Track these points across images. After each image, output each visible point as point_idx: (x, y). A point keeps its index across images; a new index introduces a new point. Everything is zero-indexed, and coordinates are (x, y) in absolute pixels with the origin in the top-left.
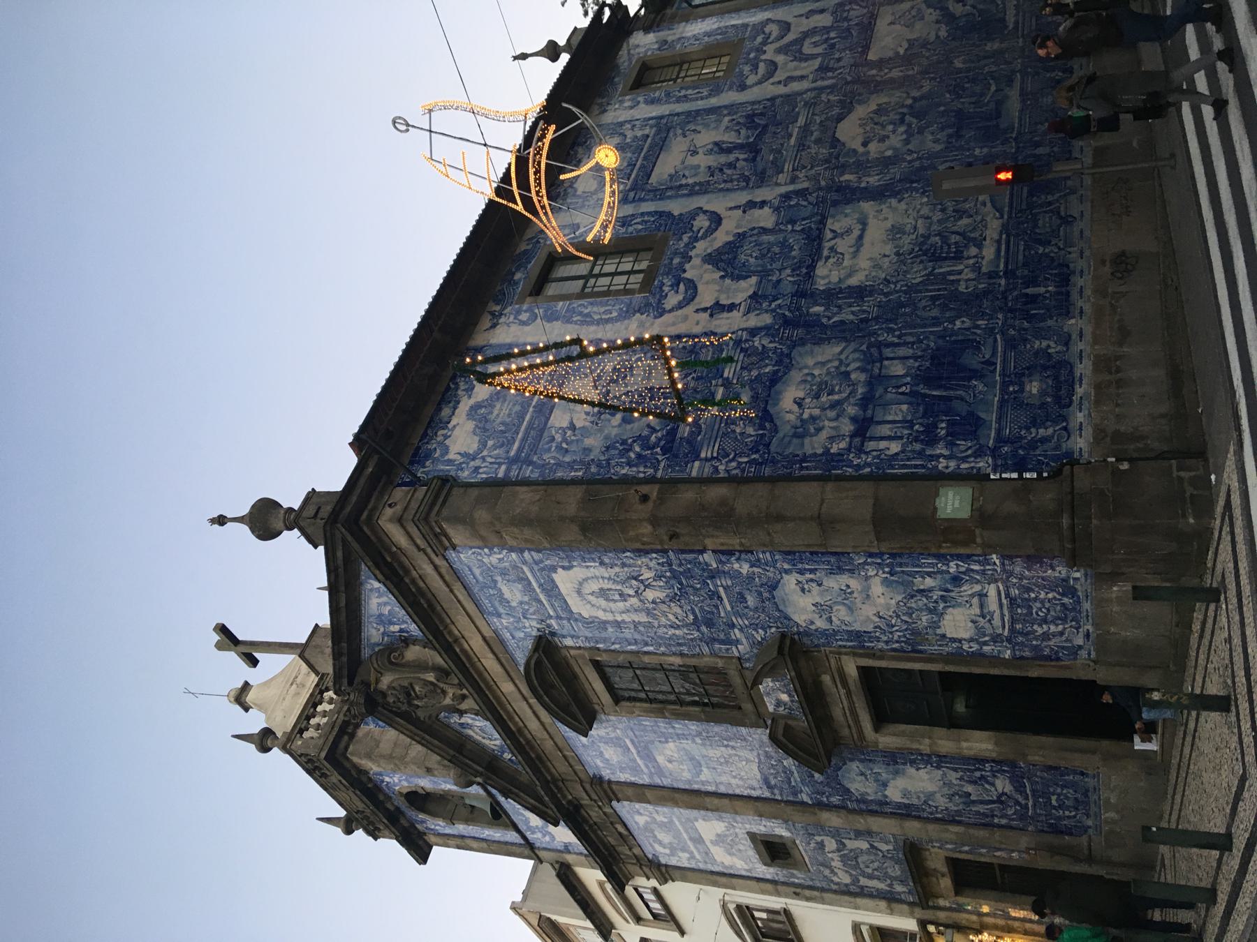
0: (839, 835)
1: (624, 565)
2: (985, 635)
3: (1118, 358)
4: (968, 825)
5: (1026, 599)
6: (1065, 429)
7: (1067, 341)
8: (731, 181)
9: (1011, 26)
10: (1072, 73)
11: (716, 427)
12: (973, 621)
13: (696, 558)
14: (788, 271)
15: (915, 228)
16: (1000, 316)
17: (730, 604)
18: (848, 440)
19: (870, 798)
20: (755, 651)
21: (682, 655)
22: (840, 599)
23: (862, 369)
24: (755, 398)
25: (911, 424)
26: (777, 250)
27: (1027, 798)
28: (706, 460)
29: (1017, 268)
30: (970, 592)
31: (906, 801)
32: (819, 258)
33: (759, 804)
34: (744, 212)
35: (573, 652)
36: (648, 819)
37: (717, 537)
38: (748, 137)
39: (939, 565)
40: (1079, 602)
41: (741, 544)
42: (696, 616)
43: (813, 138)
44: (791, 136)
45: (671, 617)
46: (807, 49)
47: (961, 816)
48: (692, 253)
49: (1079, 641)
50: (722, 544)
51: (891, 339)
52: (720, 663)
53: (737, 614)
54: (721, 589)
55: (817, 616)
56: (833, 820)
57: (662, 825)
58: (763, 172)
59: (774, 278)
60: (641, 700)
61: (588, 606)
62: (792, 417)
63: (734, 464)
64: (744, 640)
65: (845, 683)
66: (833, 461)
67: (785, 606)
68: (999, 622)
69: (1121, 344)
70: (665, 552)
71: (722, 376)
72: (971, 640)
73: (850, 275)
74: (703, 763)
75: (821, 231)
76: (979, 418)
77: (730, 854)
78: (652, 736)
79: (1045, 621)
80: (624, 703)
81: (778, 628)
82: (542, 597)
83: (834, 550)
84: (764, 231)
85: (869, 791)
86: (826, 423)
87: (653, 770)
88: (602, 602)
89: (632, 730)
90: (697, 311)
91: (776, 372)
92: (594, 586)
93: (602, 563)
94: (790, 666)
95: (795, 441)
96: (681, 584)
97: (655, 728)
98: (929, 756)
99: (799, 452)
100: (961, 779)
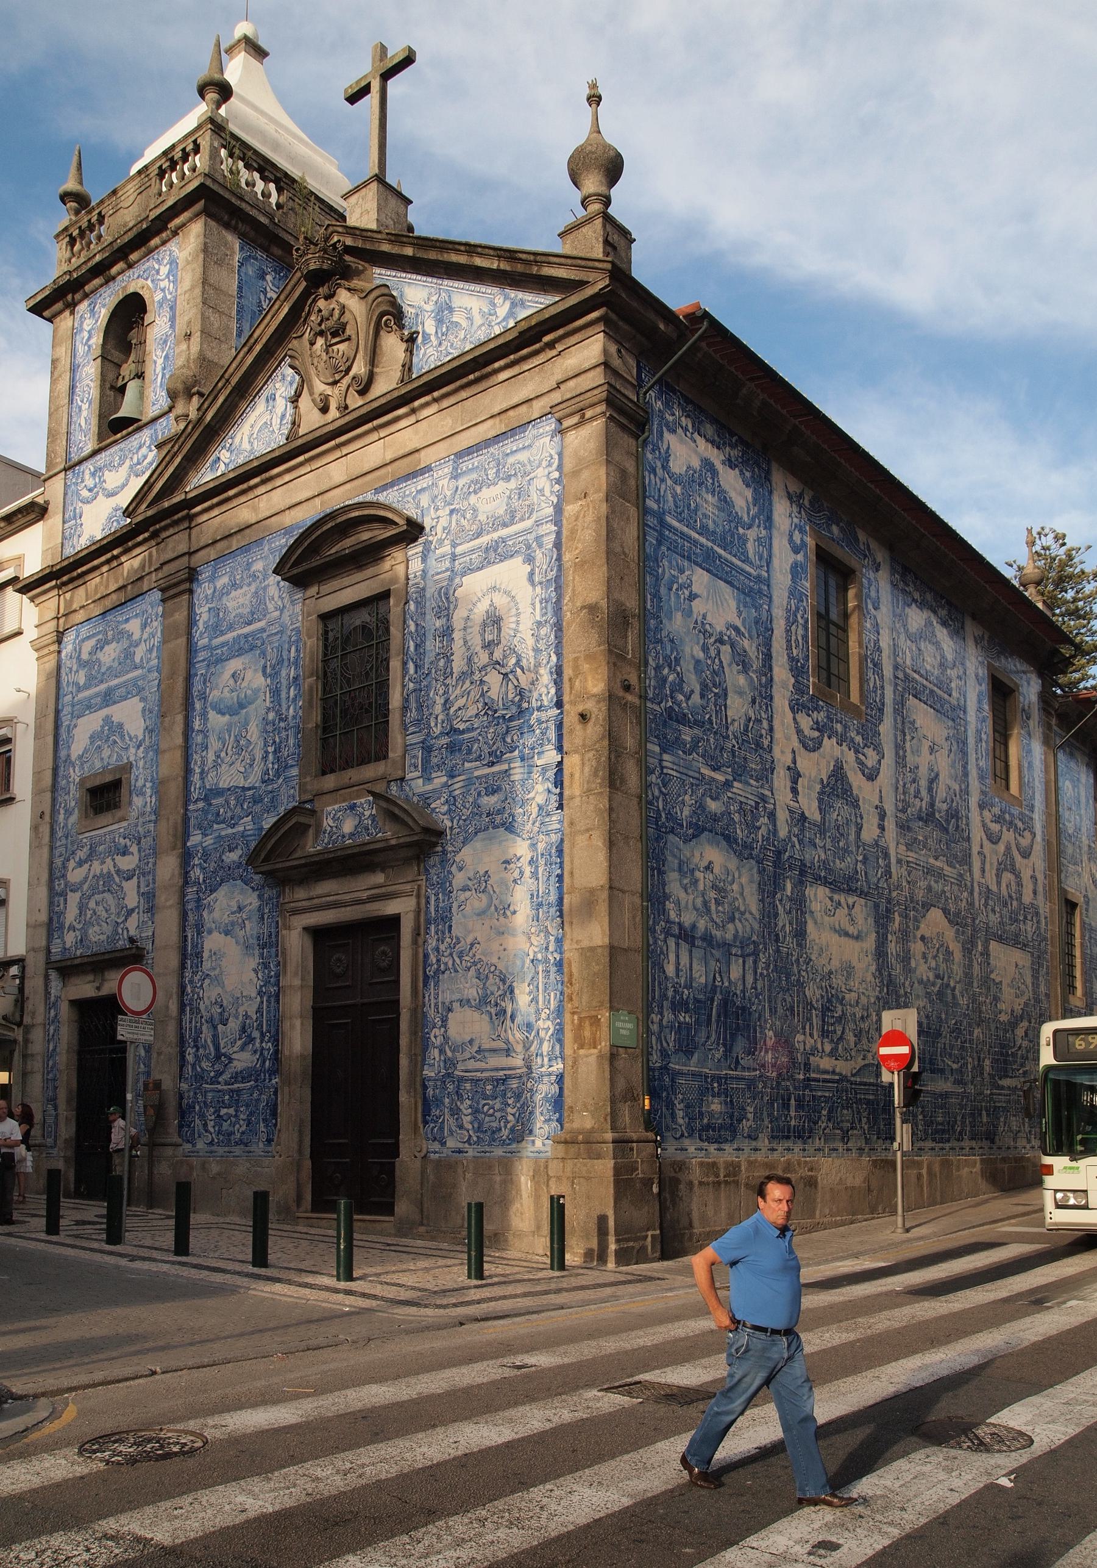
2: (453, 1051)
3: (737, 1183)
6: (682, 1135)
7: (752, 1137)
8: (904, 793)
9: (1000, 1082)
10: (958, 1140)
11: (691, 773)
12: (471, 1042)
13: (549, 741)
14: (823, 857)
15: (850, 991)
16: (774, 1074)
17: (486, 776)
18: (677, 920)
20: (415, 799)
21: (405, 709)
23: (735, 936)
24: (715, 818)
25: (689, 986)
26: (841, 844)
28: (661, 760)
29: (811, 1091)
32: (833, 891)
34: (877, 807)
36: (136, 637)
37: (582, 771)
38: (940, 812)
39: (548, 1011)
40: (503, 1143)
41: (572, 798)
42: (463, 732)
43: (932, 883)
44: (936, 859)
45: (461, 702)
46: (1007, 876)
48: (845, 747)
49: (451, 1143)
50: (572, 775)
51: (761, 965)
52: (394, 754)
53: (469, 782)
55: (471, 875)
56: (168, 867)
57: (128, 654)
58: (909, 829)
59: (817, 841)
60: (326, 647)
62: (696, 860)
63: (657, 793)
64: (429, 787)
66: (659, 903)
67: (484, 839)
68: (467, 1066)
69: (747, 1185)
71: (735, 780)
72: (446, 1038)
73: (816, 923)
75: (850, 891)
76: (692, 1054)
78: (272, 655)
79: (476, 1111)
80: (321, 626)
81: (451, 828)
84: (859, 828)
86: (692, 897)
87: (219, 651)
89: (281, 632)
90: (794, 752)
91: (736, 840)
94: (402, 840)
95: (676, 861)
96: (511, 719)
97: (286, 663)
99: (666, 868)
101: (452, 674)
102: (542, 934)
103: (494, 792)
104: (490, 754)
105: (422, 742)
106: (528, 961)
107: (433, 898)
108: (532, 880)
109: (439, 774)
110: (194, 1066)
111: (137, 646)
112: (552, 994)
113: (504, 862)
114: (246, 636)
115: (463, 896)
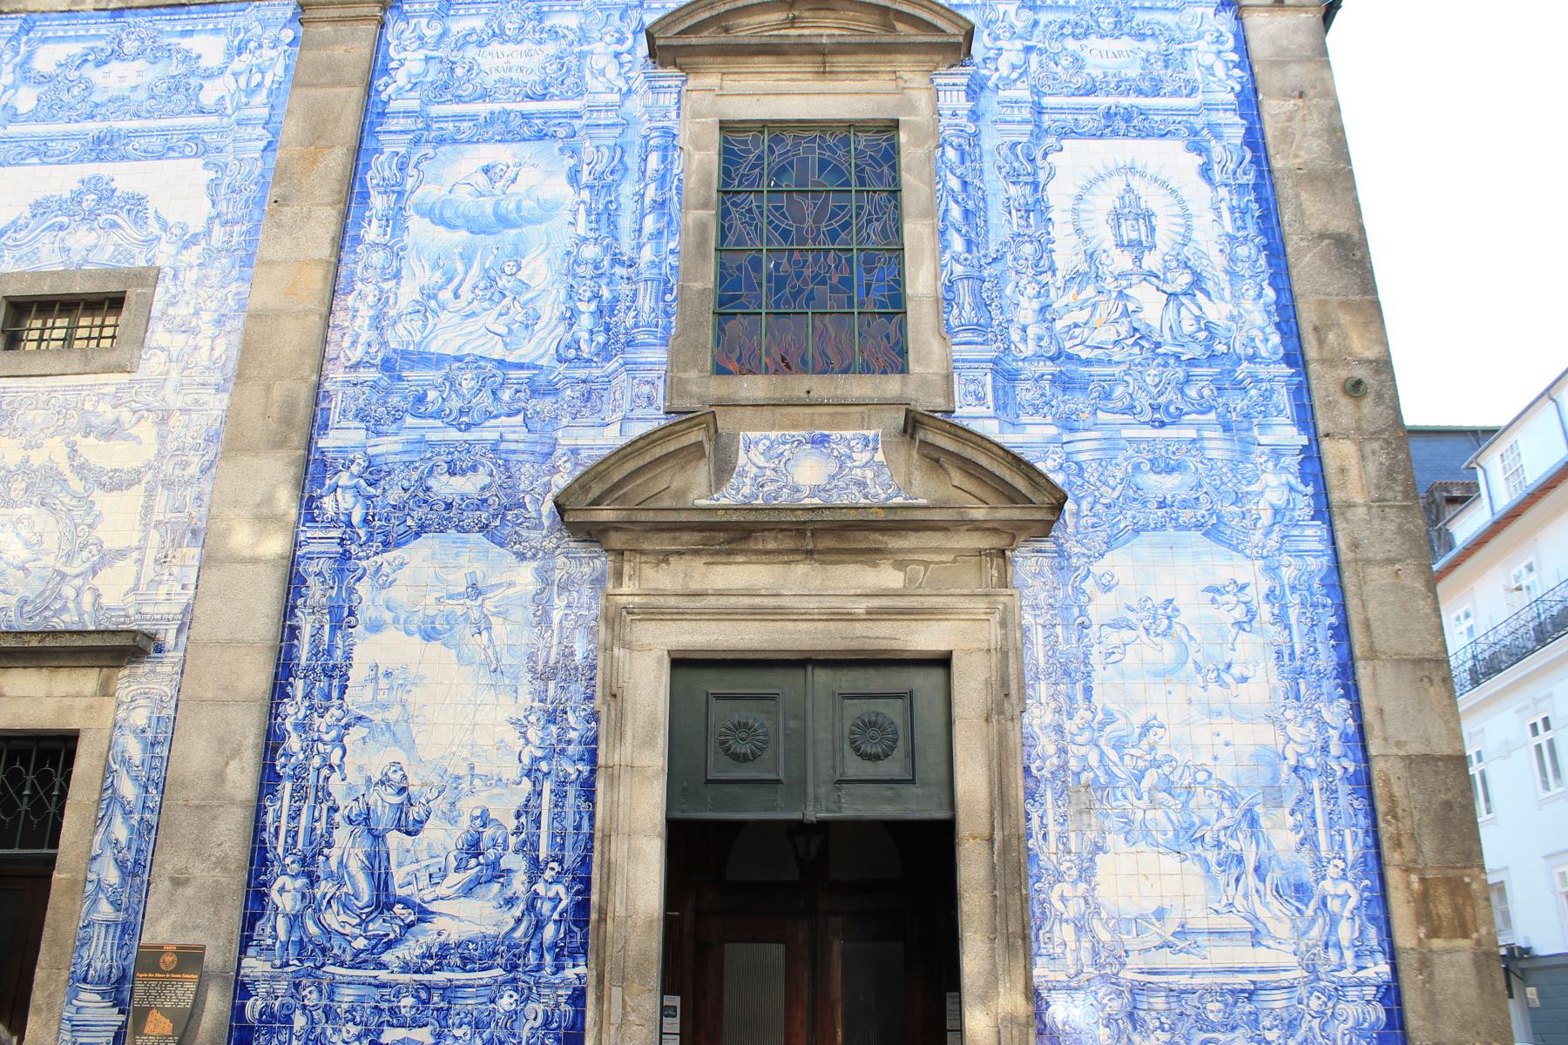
0: (168, 485)
1: (1232, 274)
4: (260, 811)
5: (1256, 1020)
12: (1160, 914)
19: (363, 588)
21: (946, 299)
22: (1193, 655)
27: (406, 968)
30: (1261, 912)
31: (356, 674)
33: (315, 321)
35: (922, 99)
39: (1342, 865)
47: (299, 793)
50: (1343, 470)
53: (1111, 446)
54: (1192, 434)
55: (1133, 603)
60: (726, 174)
61: (1092, 176)
65: (874, 615)
70: (1295, 357)
74: (490, 240)
77: (40, 209)
80: (715, 137)
82: (1102, 101)
83: (1363, 671)
85: (398, 594)
87: (451, 125)
88: (1106, 199)
92: (1153, 199)
93: (1232, 239)
96: (1192, 362)
98: (591, 756)
100: (485, 819)
101: (1053, 270)
102: (1311, 724)
103: (1170, 470)
104: (1154, 408)
105: (995, 362)
106: (1285, 771)
107: (1038, 635)
108: (1278, 628)
109: (1037, 419)
110: (295, 920)
111: (210, 75)
112: (1347, 833)
113: (1208, 590)
114: (526, 117)
115: (1115, 637)
